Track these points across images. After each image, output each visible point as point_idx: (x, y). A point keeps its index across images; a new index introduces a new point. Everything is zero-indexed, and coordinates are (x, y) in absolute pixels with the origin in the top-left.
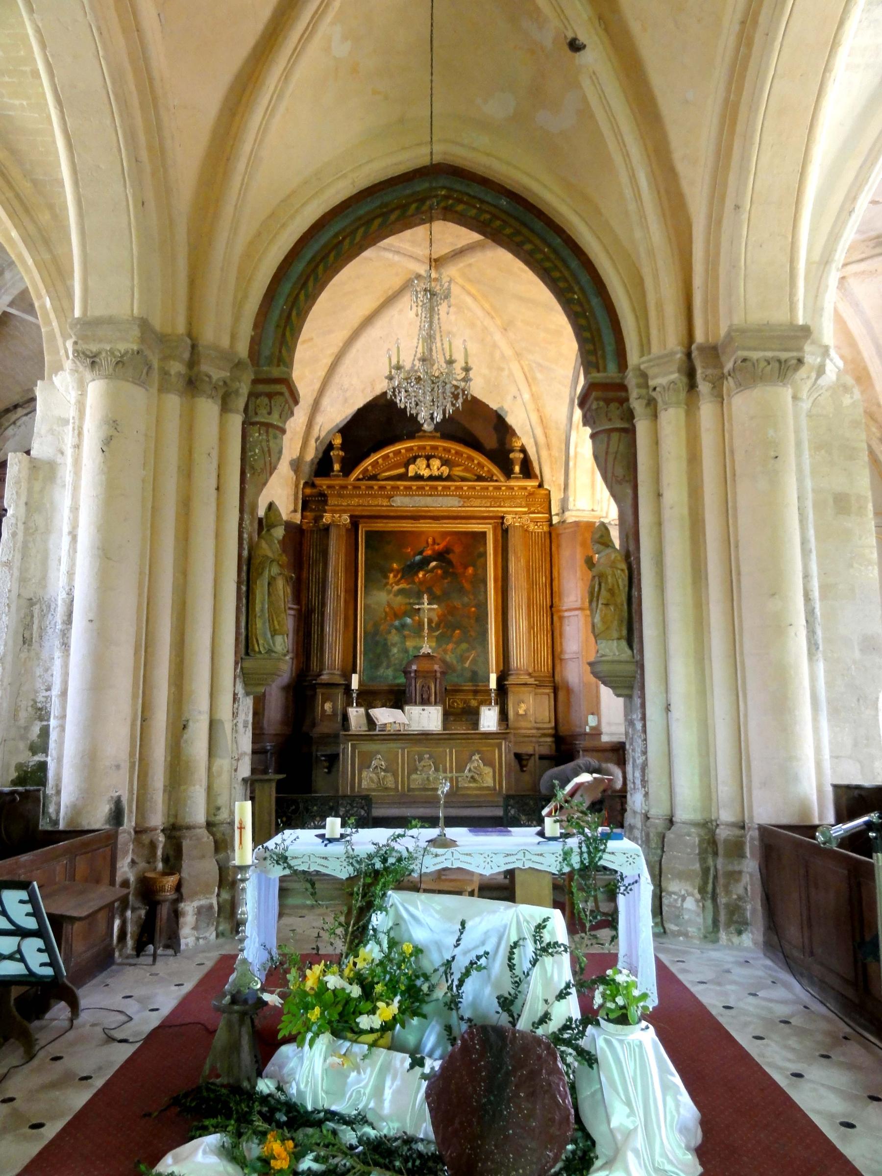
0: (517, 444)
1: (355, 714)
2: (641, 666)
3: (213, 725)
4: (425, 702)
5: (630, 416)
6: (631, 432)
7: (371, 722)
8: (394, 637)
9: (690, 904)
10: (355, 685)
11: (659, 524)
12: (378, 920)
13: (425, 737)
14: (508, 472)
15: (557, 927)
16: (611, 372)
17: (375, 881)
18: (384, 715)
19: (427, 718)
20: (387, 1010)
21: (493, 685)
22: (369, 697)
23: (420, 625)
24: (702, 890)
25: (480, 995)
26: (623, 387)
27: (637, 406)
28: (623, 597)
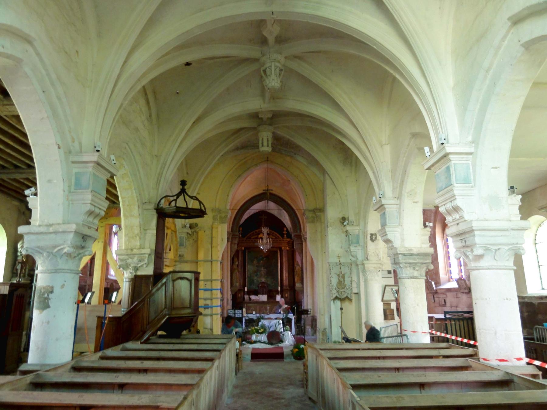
0: (285, 229)
1: (246, 297)
2: (303, 287)
3: (227, 300)
4: (263, 294)
5: (302, 241)
6: (302, 244)
7: (250, 299)
8: (255, 278)
9: (310, 330)
10: (246, 290)
11: (306, 262)
12: (260, 323)
13: (263, 302)
14: (283, 237)
15: (281, 322)
16: (298, 233)
17: (259, 319)
18: (253, 297)
19: (264, 298)
20: (262, 330)
21: (279, 289)
22: (250, 293)
23: (262, 275)
24: (312, 327)
25: (271, 330)
26: (301, 236)
27: (303, 240)
28: (301, 275)
